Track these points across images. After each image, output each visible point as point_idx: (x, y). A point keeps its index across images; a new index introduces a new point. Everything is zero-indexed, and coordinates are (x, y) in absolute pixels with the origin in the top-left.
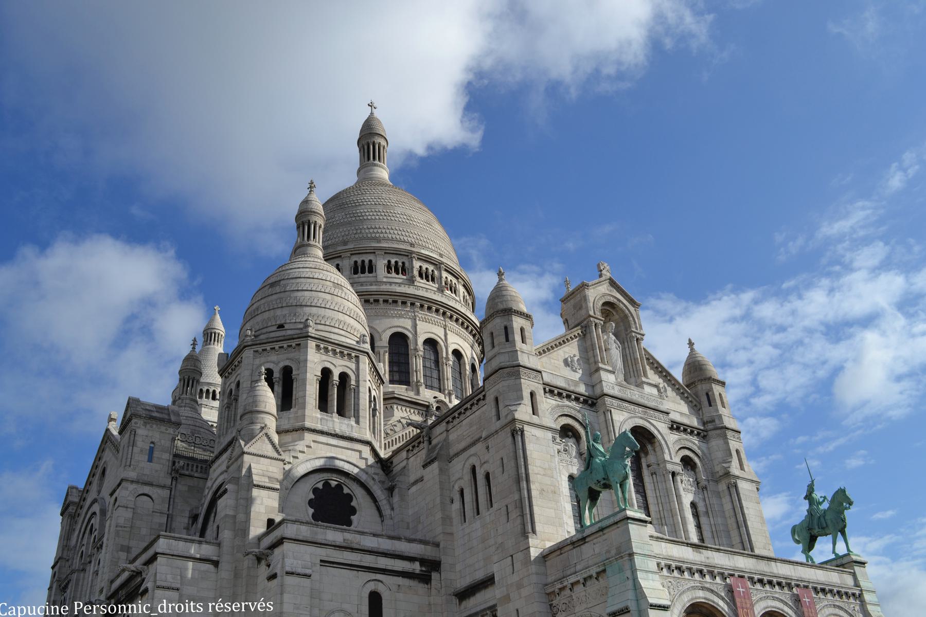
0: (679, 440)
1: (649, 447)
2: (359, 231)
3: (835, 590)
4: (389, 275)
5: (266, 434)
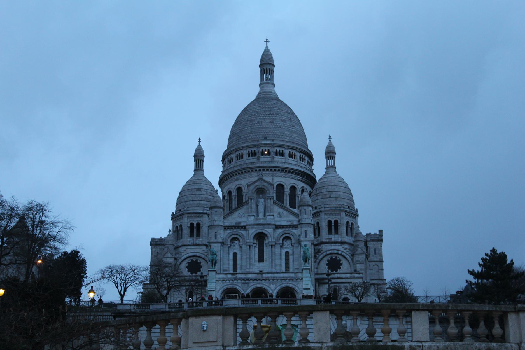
0: (283, 231)
1: (266, 238)
3: (289, 279)
4: (249, 158)
5: (168, 251)
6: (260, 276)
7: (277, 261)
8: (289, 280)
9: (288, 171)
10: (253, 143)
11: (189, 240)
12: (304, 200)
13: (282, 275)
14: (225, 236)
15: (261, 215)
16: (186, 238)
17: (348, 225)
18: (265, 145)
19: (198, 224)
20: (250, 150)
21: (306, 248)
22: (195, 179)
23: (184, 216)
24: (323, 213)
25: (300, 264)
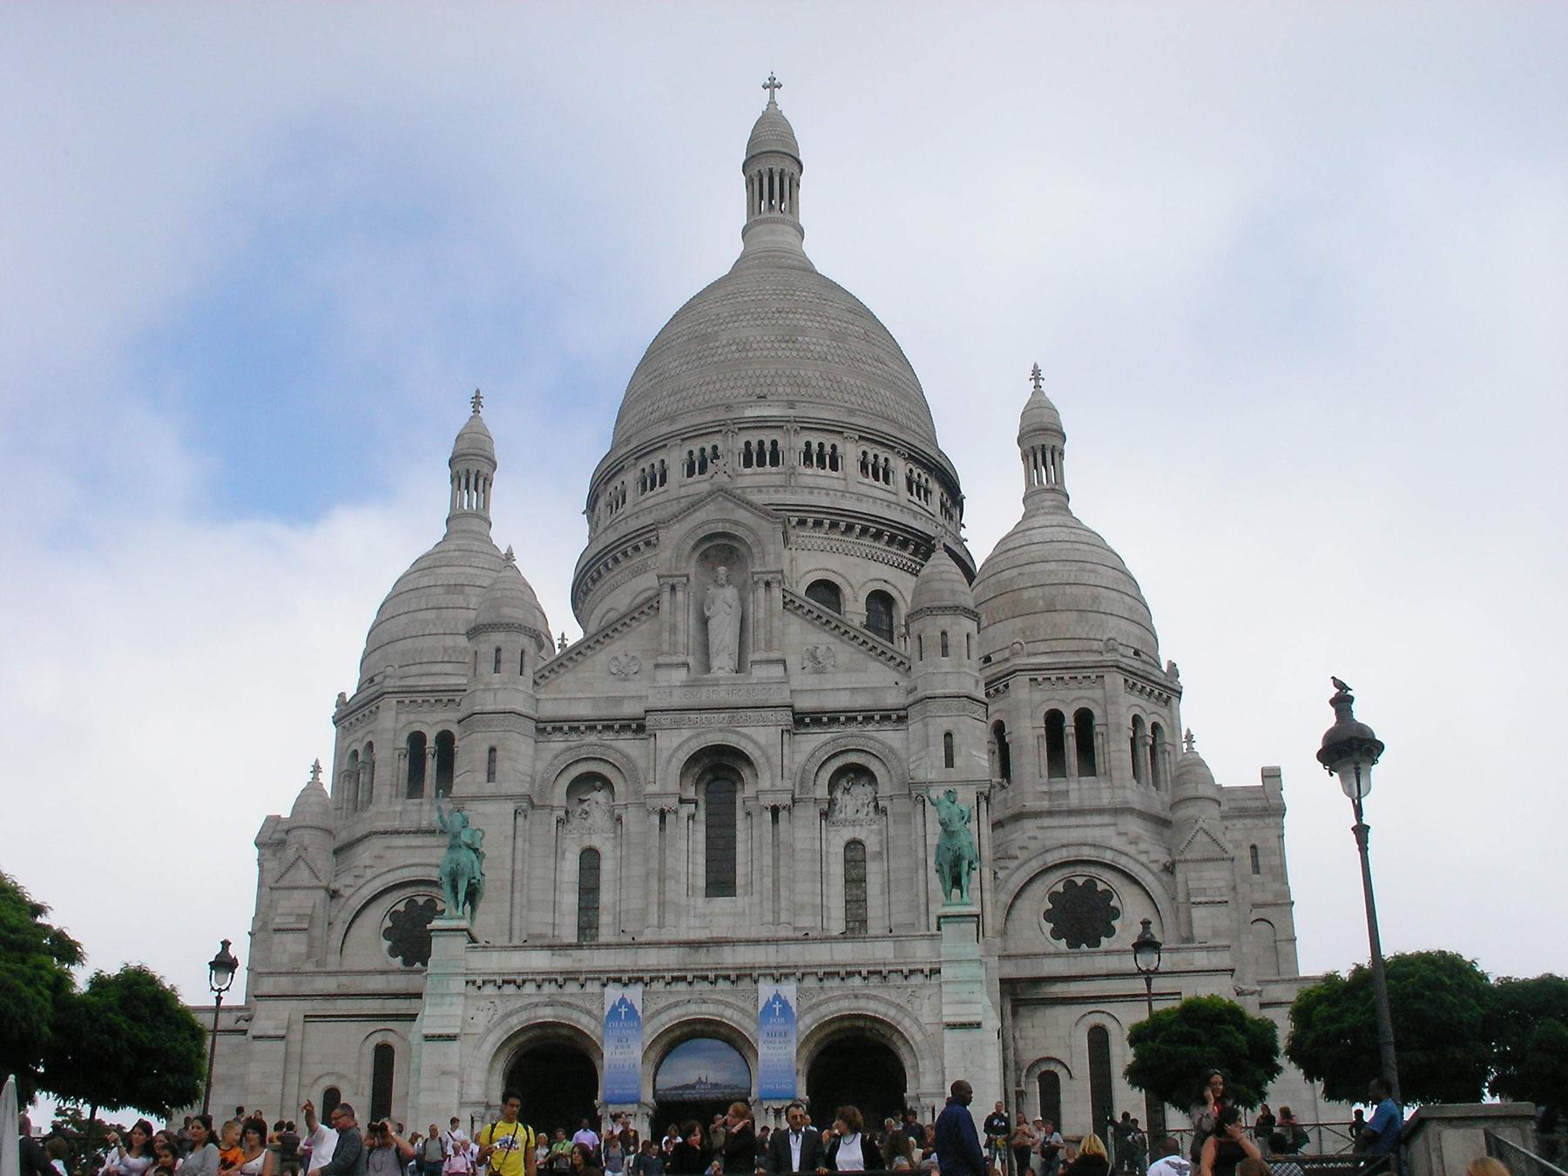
0: (833, 741)
1: (746, 773)
2: (656, 407)
3: (864, 972)
6: (704, 959)
7: (805, 890)
8: (865, 978)
9: (858, 528)
10: (709, 418)
11: (399, 808)
12: (936, 585)
13: (820, 954)
14: (540, 766)
15: (723, 663)
16: (385, 798)
17: (1139, 734)
18: (761, 424)
19: (446, 740)
20: (695, 446)
21: (955, 809)
22: (447, 548)
23: (381, 704)
24: (1023, 679)
25: (922, 900)
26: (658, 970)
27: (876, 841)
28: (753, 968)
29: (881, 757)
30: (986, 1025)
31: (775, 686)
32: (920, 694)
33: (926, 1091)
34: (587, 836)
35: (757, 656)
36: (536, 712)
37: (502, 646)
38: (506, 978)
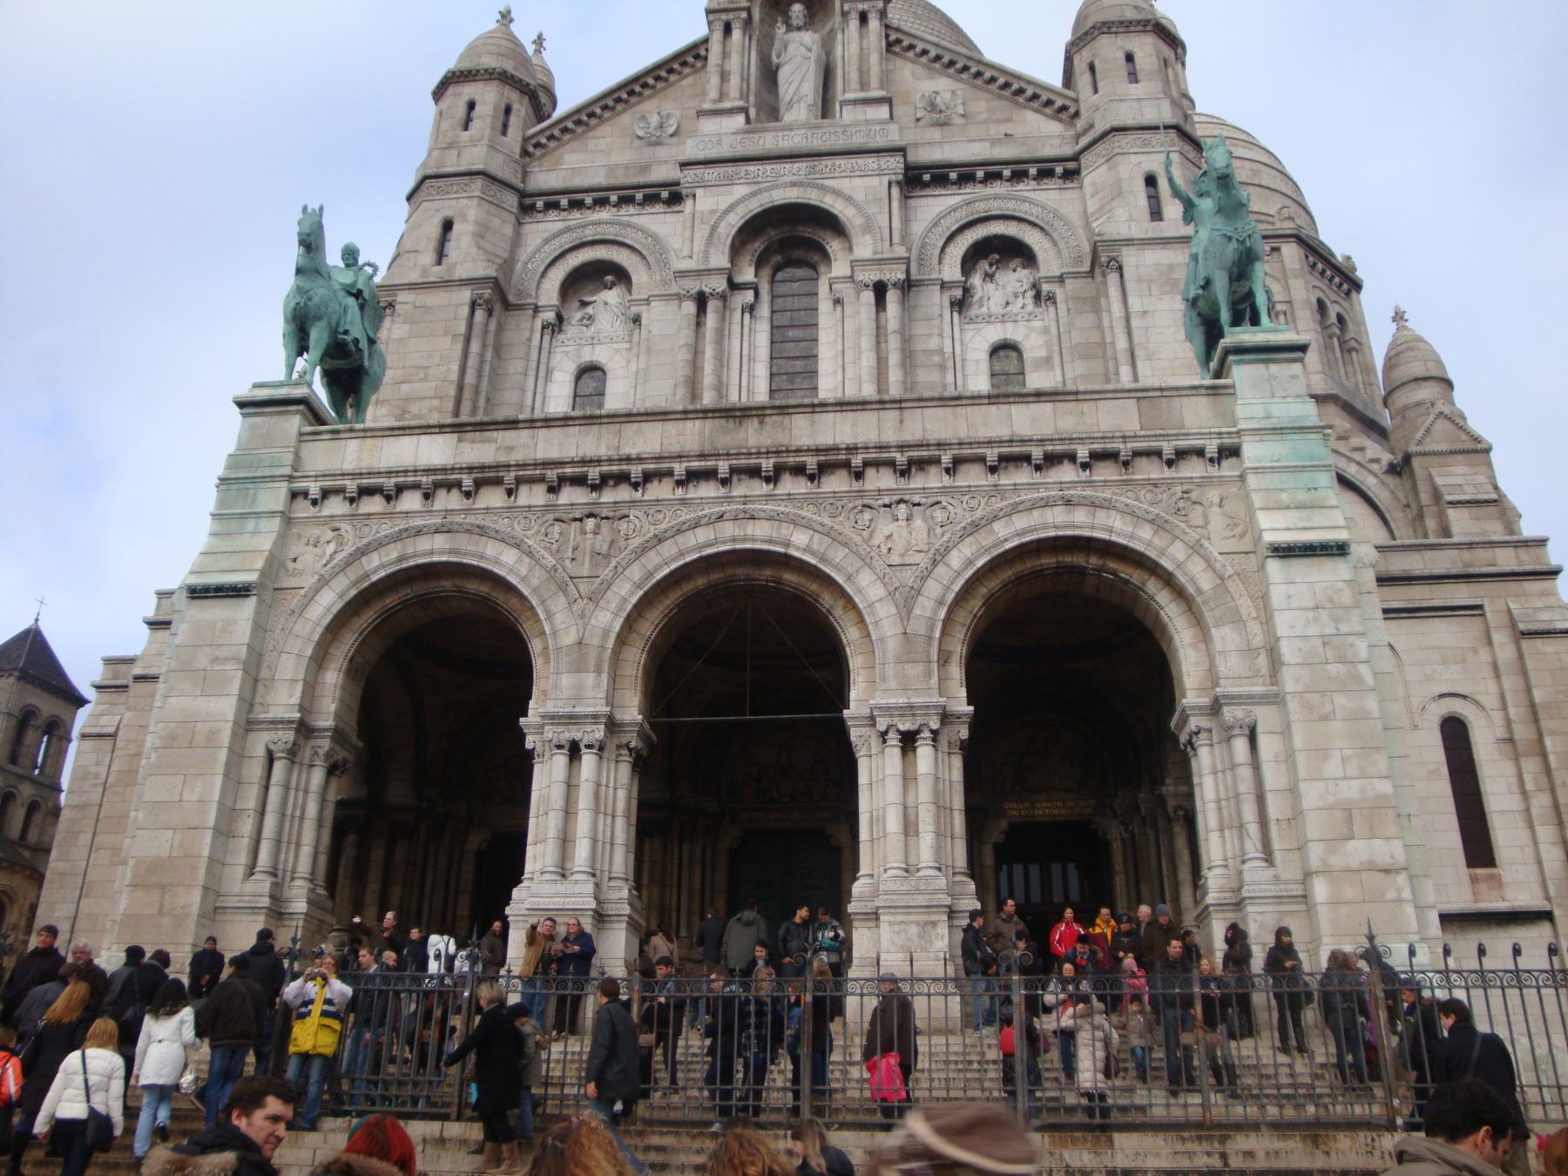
1: (834, 246)
3: (1083, 453)
26: (659, 458)
27: (1041, 342)
28: (852, 449)
29: (1041, 224)
30: (1354, 549)
31: (878, 128)
32: (1100, 128)
33: (1235, 690)
34: (587, 349)
35: (850, 96)
36: (523, 181)
37: (477, 98)
38: (365, 481)
